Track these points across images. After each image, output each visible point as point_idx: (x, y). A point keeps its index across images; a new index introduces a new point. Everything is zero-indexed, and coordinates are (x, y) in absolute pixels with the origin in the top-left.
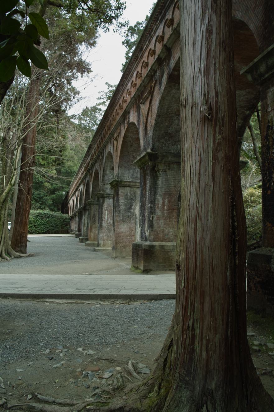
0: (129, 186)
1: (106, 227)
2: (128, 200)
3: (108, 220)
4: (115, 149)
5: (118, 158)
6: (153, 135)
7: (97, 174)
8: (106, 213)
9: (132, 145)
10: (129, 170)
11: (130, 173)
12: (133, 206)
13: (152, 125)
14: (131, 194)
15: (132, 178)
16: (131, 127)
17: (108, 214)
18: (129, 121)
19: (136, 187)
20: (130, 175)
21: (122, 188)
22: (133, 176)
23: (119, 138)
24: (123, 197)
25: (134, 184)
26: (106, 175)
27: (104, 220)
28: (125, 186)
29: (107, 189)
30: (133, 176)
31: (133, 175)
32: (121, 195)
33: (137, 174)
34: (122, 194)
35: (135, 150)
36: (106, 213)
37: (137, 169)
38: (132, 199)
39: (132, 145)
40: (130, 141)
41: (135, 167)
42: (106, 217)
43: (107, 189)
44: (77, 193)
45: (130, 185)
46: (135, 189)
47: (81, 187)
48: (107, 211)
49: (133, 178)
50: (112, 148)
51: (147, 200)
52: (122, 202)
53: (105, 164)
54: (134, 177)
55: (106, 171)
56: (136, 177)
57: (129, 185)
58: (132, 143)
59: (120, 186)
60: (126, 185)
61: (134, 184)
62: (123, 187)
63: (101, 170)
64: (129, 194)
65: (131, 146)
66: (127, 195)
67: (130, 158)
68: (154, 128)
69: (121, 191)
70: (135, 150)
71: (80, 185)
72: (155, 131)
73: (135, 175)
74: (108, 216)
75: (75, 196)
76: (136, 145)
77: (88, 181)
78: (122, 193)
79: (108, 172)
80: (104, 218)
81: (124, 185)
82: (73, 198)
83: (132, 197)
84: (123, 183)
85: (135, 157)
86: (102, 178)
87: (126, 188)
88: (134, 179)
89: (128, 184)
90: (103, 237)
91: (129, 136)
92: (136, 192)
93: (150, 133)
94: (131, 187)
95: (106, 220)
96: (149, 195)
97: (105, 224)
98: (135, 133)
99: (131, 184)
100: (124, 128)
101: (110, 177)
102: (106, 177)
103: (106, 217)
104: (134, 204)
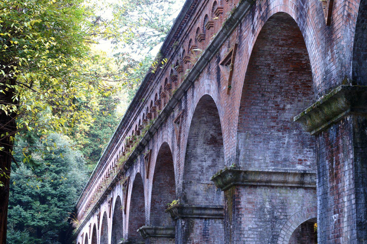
0: (268, 185)
2: (265, 221)
4: (224, 88)
5: (237, 111)
6: (356, 40)
7: (166, 155)
9: (273, 76)
10: (267, 140)
11: (268, 149)
12: (280, 239)
13: (349, 15)
14: (273, 206)
15: (275, 163)
16: (274, 26)
18: (268, 10)
19: (286, 187)
20: (269, 154)
21: (249, 190)
22: (276, 156)
23: (237, 55)
24: (252, 213)
25: (281, 178)
26: (195, 157)
28: (254, 185)
30: (276, 156)
31: (276, 154)
32: (246, 209)
33: (287, 151)
34: (250, 206)
35: (281, 88)
37: (287, 140)
38: (276, 218)
39: (273, 76)
40: (269, 65)
41: (280, 134)
44: (104, 208)
45: (270, 181)
46: (283, 191)
47: (118, 192)
49: (278, 162)
50: (214, 87)
51: (345, 219)
52: (250, 229)
53: (191, 129)
54: (279, 159)
55: (194, 147)
56: (285, 160)
57: (267, 182)
58: (273, 70)
59: (244, 186)
60: (260, 181)
61: (281, 178)
62: (251, 186)
63: (179, 145)
64: (268, 206)
65: (271, 77)
66: (262, 209)
67: (266, 110)
68: (358, 21)
69: (246, 198)
70: (281, 88)
71: (113, 186)
72: (360, 31)
73: (283, 154)
75: (99, 216)
76: (283, 76)
77: (138, 175)
78: (249, 203)
79: (199, 151)
81: (254, 181)
82: (94, 220)
83: (276, 214)
84: (251, 177)
85: (281, 106)
86: (182, 166)
87: (259, 190)
88: (279, 167)
89: (265, 178)
91: (266, 53)
92: (286, 198)
93: (345, 35)
94: (273, 187)
96: (351, 205)
98: (281, 42)
99: (274, 178)
100: (253, 31)
101: (204, 164)
102: (193, 163)
104: (282, 232)
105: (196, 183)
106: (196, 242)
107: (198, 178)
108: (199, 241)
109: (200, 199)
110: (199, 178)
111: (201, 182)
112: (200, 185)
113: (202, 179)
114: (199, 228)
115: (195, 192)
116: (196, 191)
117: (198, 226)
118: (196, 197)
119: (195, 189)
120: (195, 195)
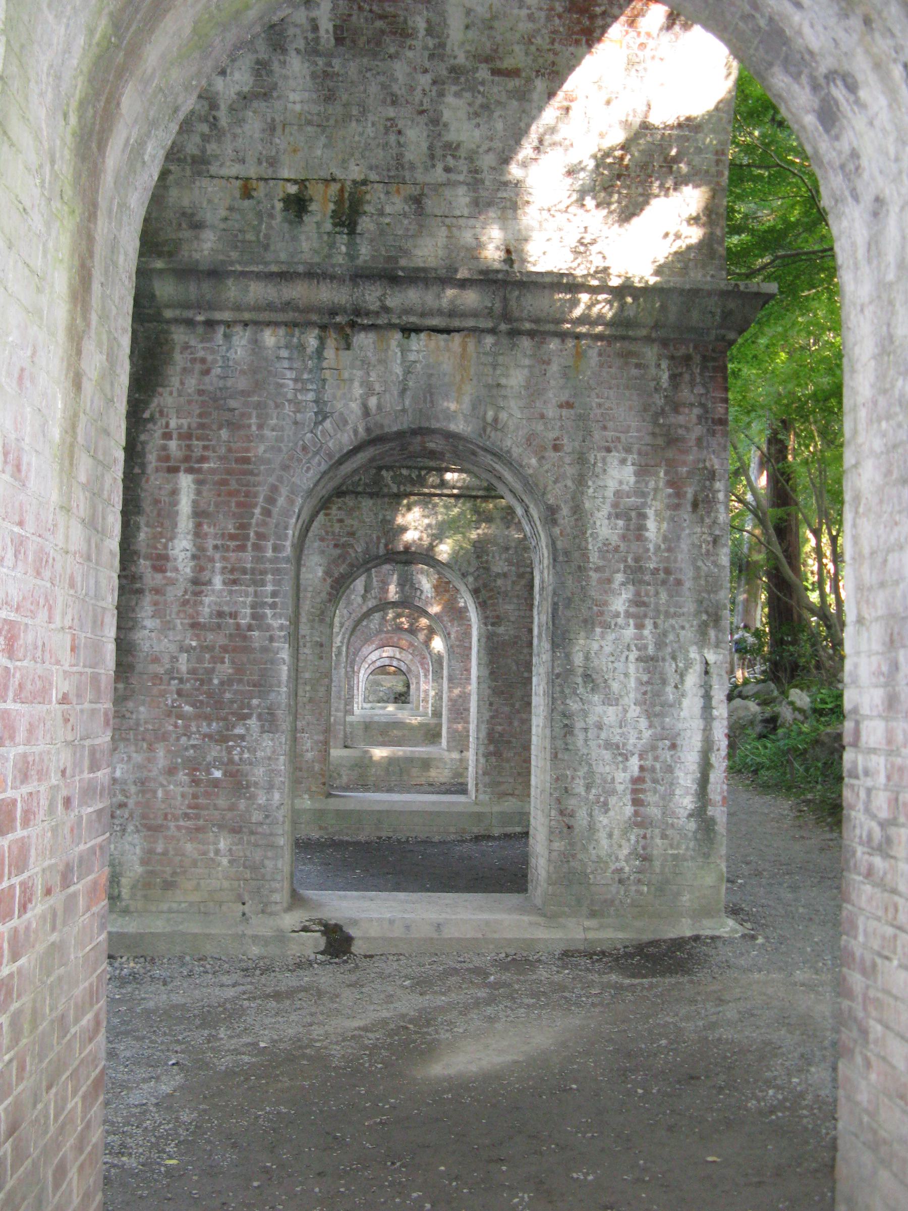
1: (183, 664)
3: (198, 583)
8: (185, 506)
17: (199, 514)
27: (151, 579)
29: (198, 226)
36: (185, 506)
42: (181, 547)
43: (198, 226)
48: (186, 481)
74: (198, 533)
80: (161, 562)
90: (142, 782)
95: (174, 593)
97: (168, 626)
103: (181, 547)
105: (188, 173)
106: (180, 427)
107: (196, 152)
108: (194, 425)
109: (207, 246)
110: (203, 151)
111: (213, 169)
112: (205, 182)
113: (216, 157)
114: (198, 367)
115: (184, 214)
116: (189, 211)
117: (194, 361)
118: (187, 234)
119: (186, 202)
120: (184, 226)
